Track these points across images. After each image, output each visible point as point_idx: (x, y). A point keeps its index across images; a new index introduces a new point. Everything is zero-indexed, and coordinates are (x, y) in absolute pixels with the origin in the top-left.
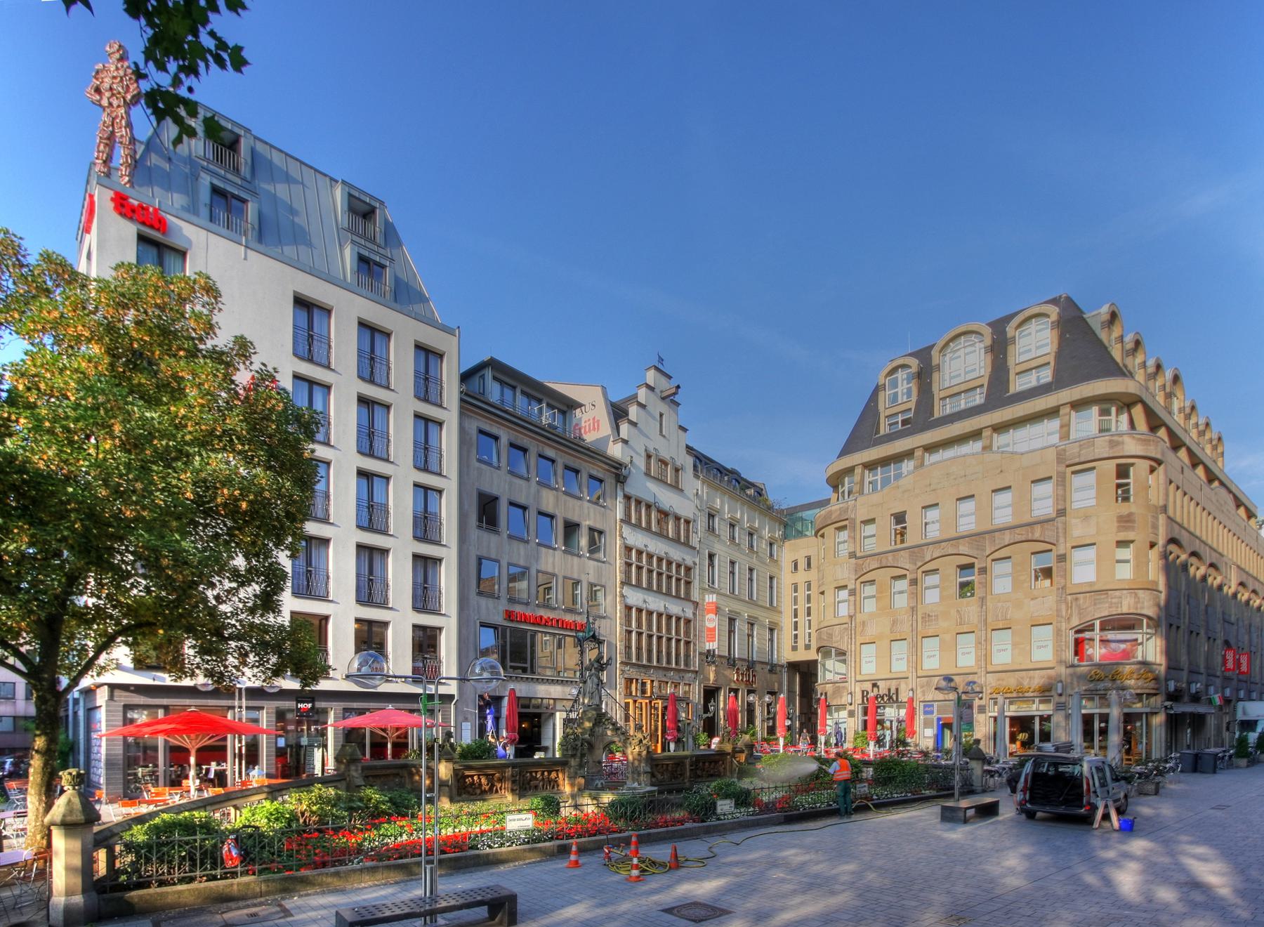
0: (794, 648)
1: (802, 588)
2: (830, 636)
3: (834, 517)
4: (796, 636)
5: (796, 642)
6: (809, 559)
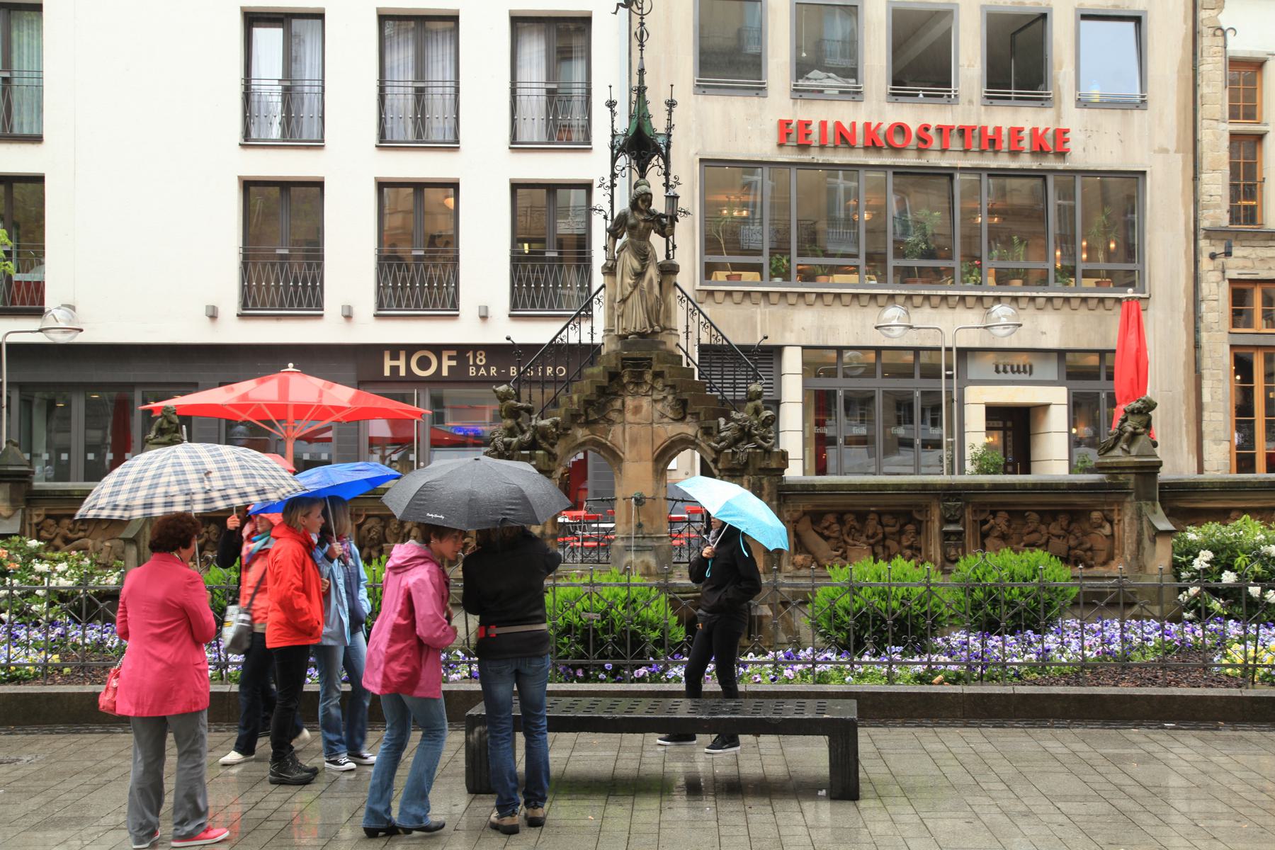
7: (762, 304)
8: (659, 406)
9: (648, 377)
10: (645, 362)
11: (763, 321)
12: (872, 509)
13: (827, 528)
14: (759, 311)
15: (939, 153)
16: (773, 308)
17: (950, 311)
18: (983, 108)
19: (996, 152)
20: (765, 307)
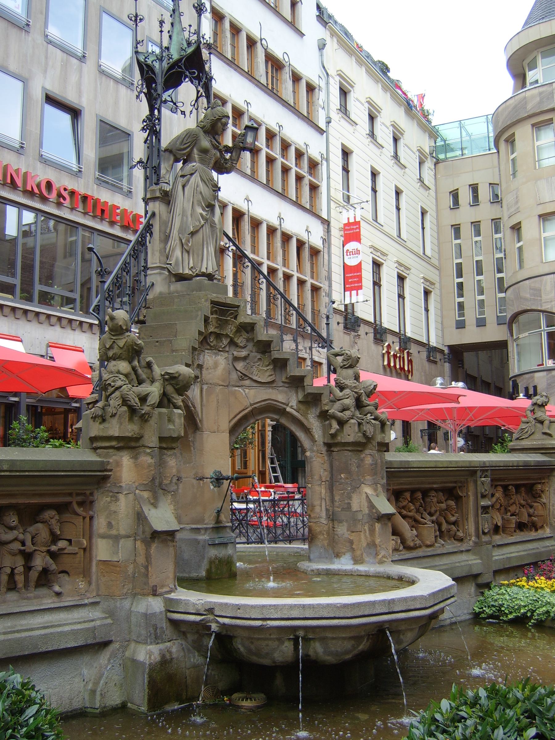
0: (461, 325)
1: (466, 231)
2: (537, 292)
3: (531, 107)
4: (461, 306)
5: (462, 315)
6: (474, 188)
8: (240, 366)
10: (232, 310)
12: (435, 486)
13: (404, 507)
15: (69, 210)
17: (72, 332)
18: (95, 186)
19: (102, 219)
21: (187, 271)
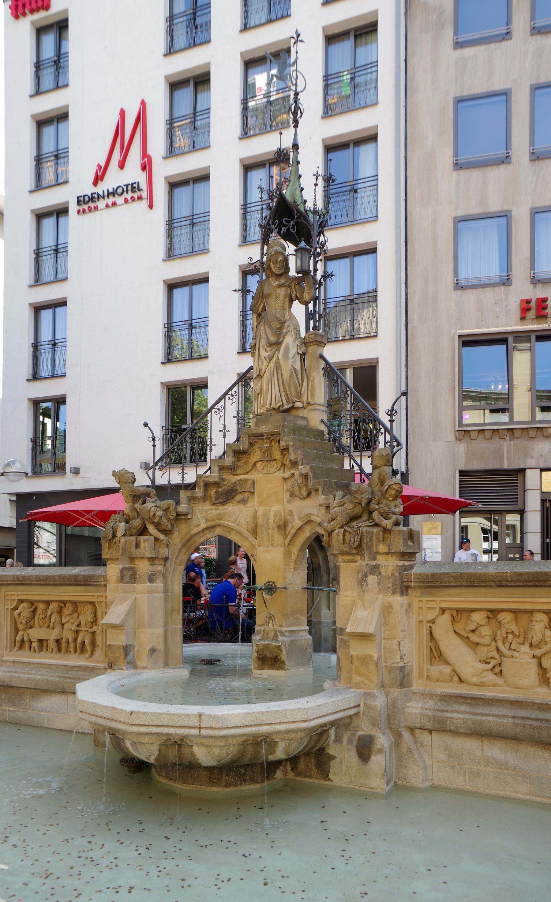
7: (508, 438)
9: (277, 454)
11: (509, 451)
14: (505, 444)
16: (517, 441)
20: (510, 440)
21: (259, 412)
